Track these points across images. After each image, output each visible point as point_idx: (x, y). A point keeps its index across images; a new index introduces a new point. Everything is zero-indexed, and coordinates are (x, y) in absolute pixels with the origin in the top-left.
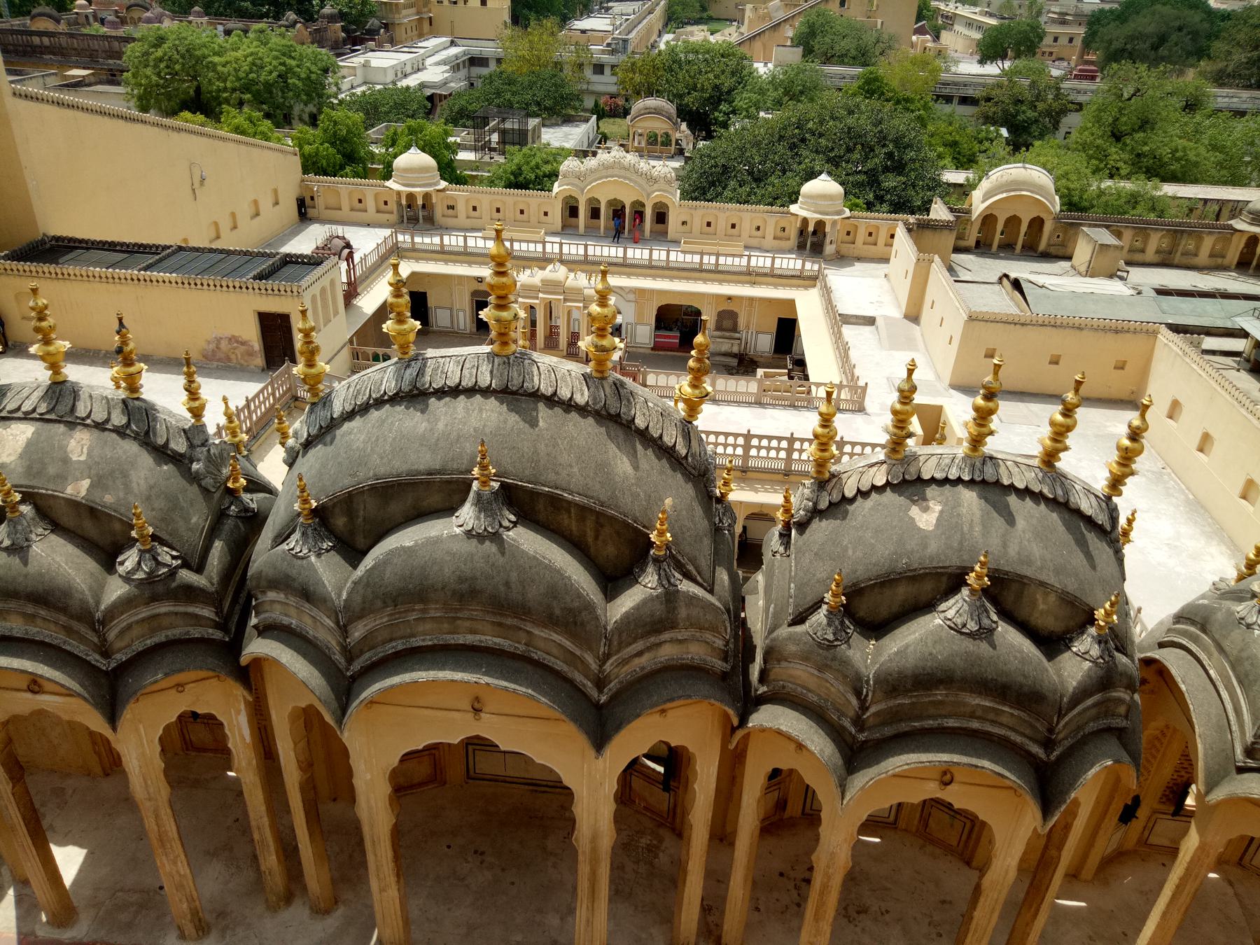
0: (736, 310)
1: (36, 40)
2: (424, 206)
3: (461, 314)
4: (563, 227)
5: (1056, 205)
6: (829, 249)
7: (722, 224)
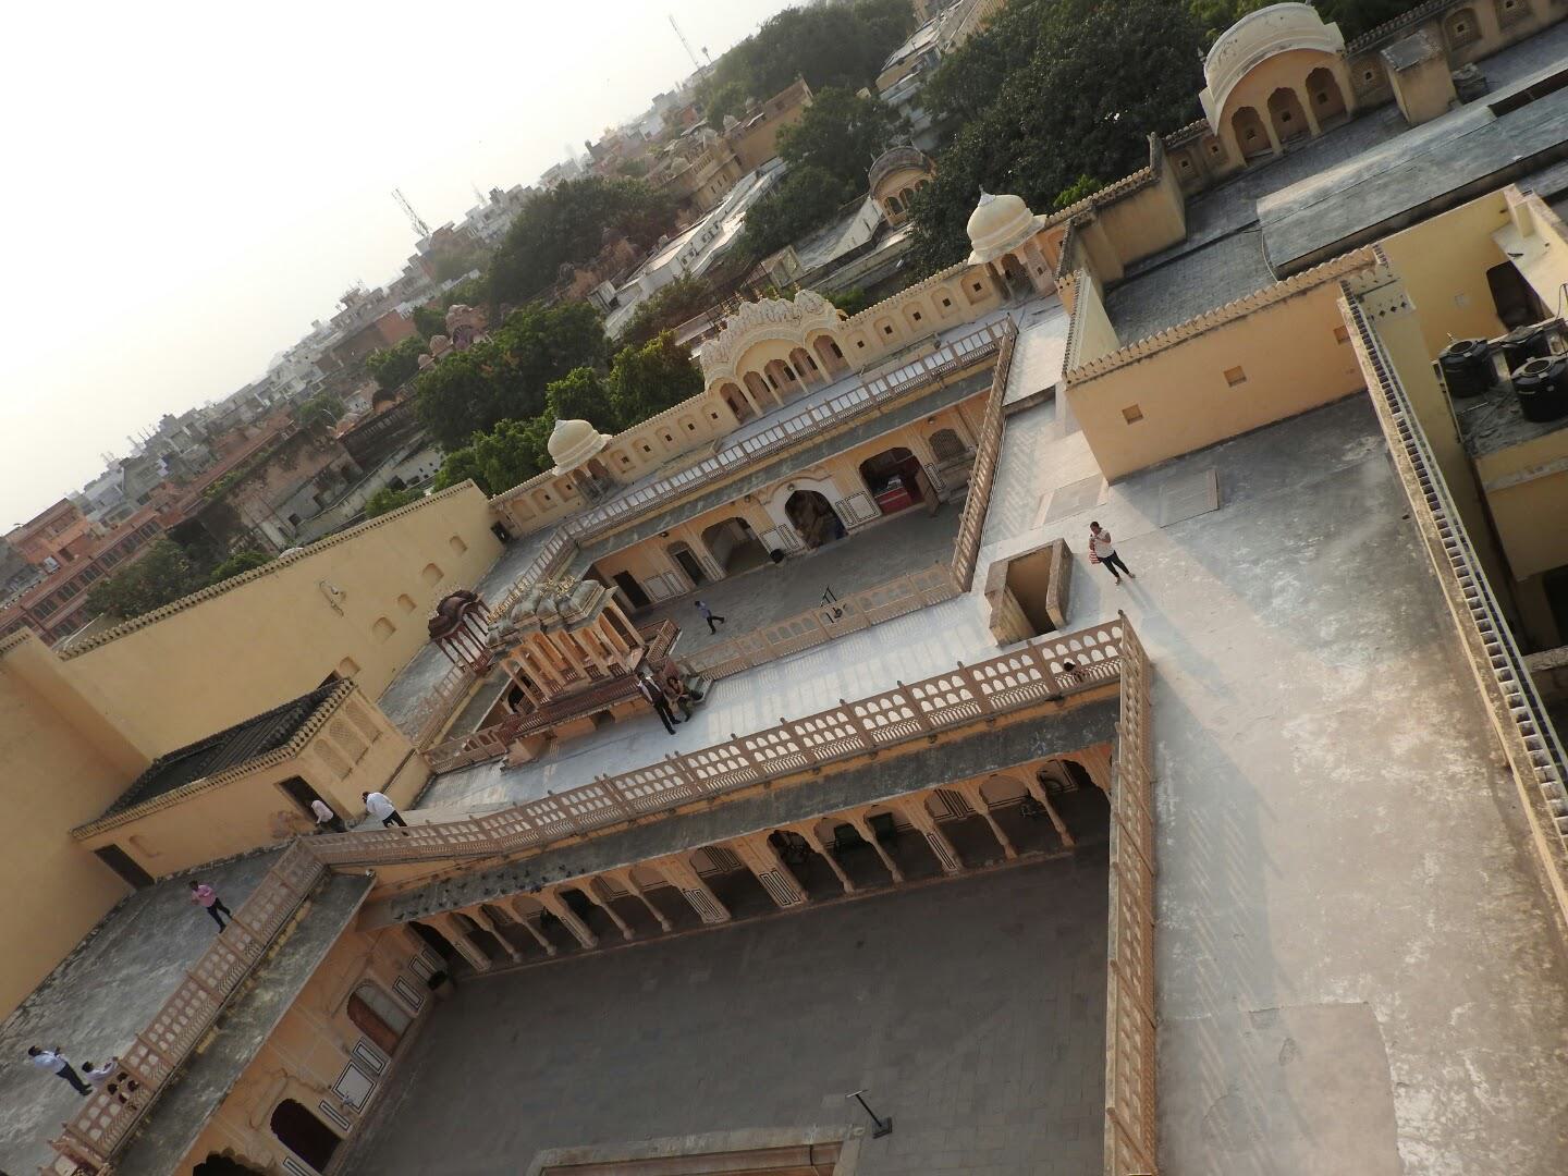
0: (946, 426)
1: (381, 425)
2: (594, 477)
3: (670, 576)
4: (741, 421)
5: (1329, 37)
6: (1041, 283)
7: (900, 321)
